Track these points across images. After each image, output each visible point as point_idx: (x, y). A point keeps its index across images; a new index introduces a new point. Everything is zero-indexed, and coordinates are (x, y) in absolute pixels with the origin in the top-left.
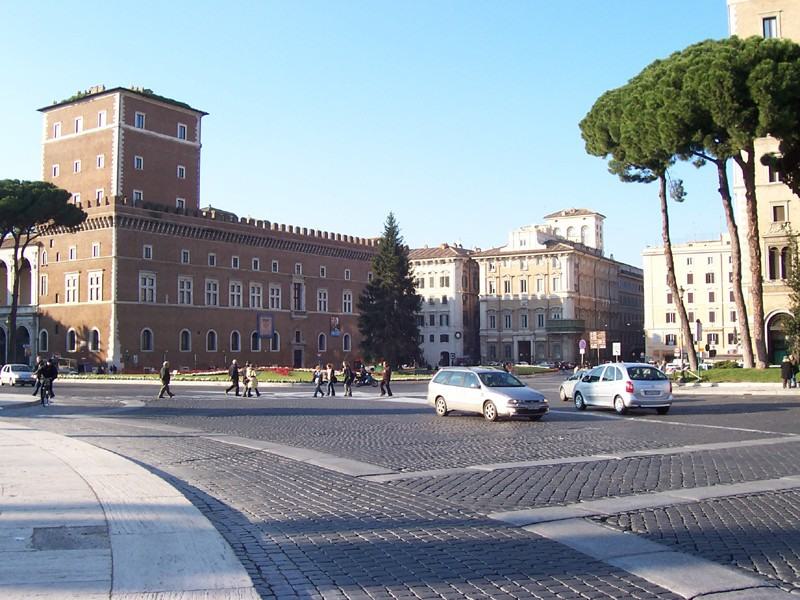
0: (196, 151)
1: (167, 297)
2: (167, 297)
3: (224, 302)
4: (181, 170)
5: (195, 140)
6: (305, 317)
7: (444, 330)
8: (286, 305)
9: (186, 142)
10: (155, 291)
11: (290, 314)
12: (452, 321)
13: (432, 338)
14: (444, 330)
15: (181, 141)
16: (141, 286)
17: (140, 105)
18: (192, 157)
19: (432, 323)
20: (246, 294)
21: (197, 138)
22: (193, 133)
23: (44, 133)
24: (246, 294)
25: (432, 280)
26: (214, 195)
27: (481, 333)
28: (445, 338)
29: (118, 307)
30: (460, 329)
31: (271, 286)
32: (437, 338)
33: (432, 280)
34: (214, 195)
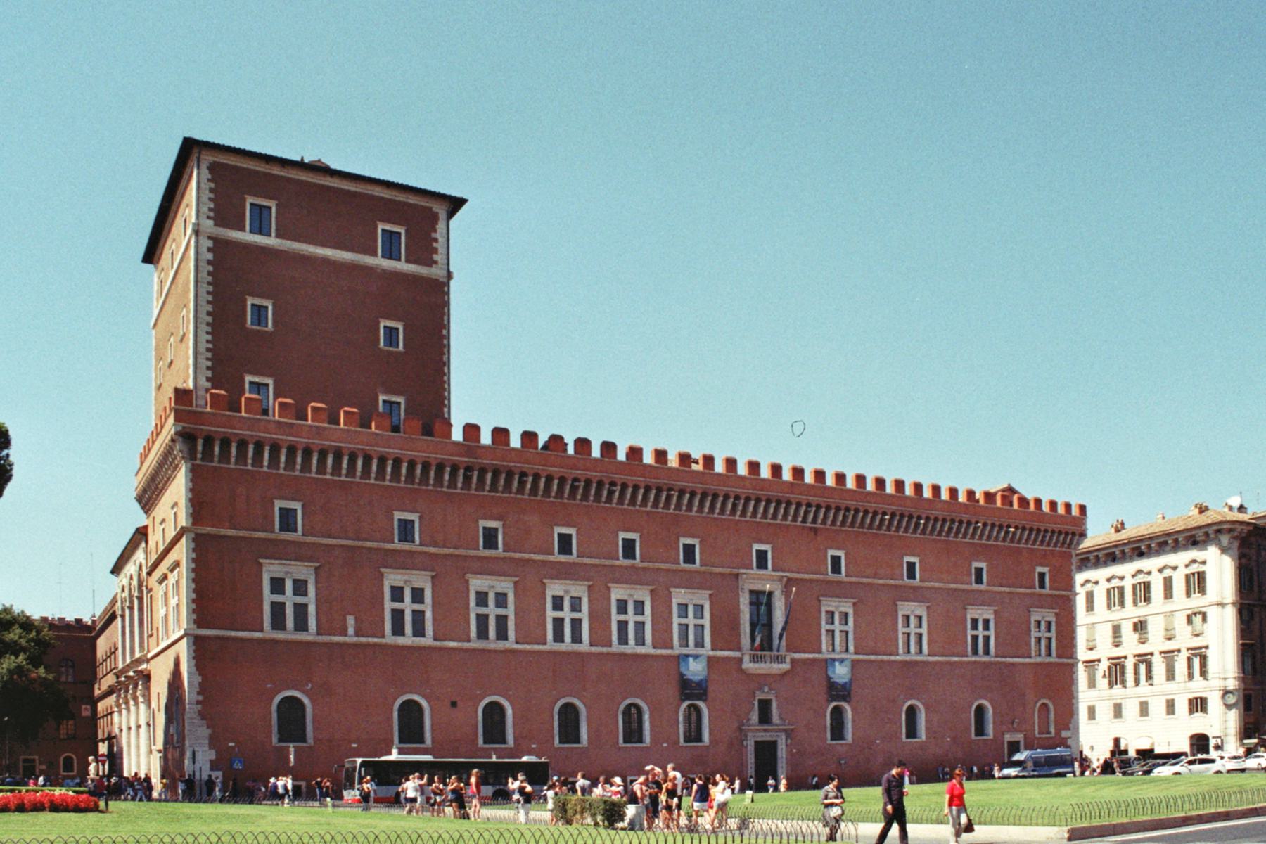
1: (351, 620)
2: (351, 620)
3: (531, 632)
4: (391, 332)
5: (432, 263)
6: (786, 666)
7: (1198, 687)
10: (312, 609)
11: (740, 660)
14: (1198, 687)
16: (268, 597)
17: (222, 175)
18: (427, 306)
19: (1171, 675)
20: (662, 622)
24: (662, 622)
26: (489, 391)
28: (1198, 705)
30: (1232, 684)
31: (679, 596)
32: (1182, 706)
34: (489, 391)
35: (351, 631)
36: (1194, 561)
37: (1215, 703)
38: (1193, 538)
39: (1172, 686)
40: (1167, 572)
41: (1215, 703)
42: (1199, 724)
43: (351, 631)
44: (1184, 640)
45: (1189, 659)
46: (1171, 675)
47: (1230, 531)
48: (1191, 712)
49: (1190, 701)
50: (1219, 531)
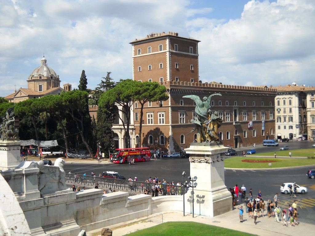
0: (196, 57)
7: (291, 123)
8: (231, 120)
9: (193, 54)
12: (294, 120)
13: (285, 127)
15: (191, 54)
19: (285, 121)
21: (197, 52)
22: (195, 50)
23: (133, 53)
25: (284, 101)
27: (308, 125)
28: (291, 127)
29: (172, 126)
30: (298, 123)
32: (287, 127)
33: (284, 101)
35: (189, 122)
36: (290, 98)
37: (294, 127)
38: (290, 93)
39: (285, 123)
40: (284, 99)
41: (294, 127)
42: (291, 131)
43: (189, 122)
44: (288, 114)
45: (289, 118)
46: (285, 121)
47: (298, 92)
48: (289, 129)
49: (289, 126)
50: (295, 92)
